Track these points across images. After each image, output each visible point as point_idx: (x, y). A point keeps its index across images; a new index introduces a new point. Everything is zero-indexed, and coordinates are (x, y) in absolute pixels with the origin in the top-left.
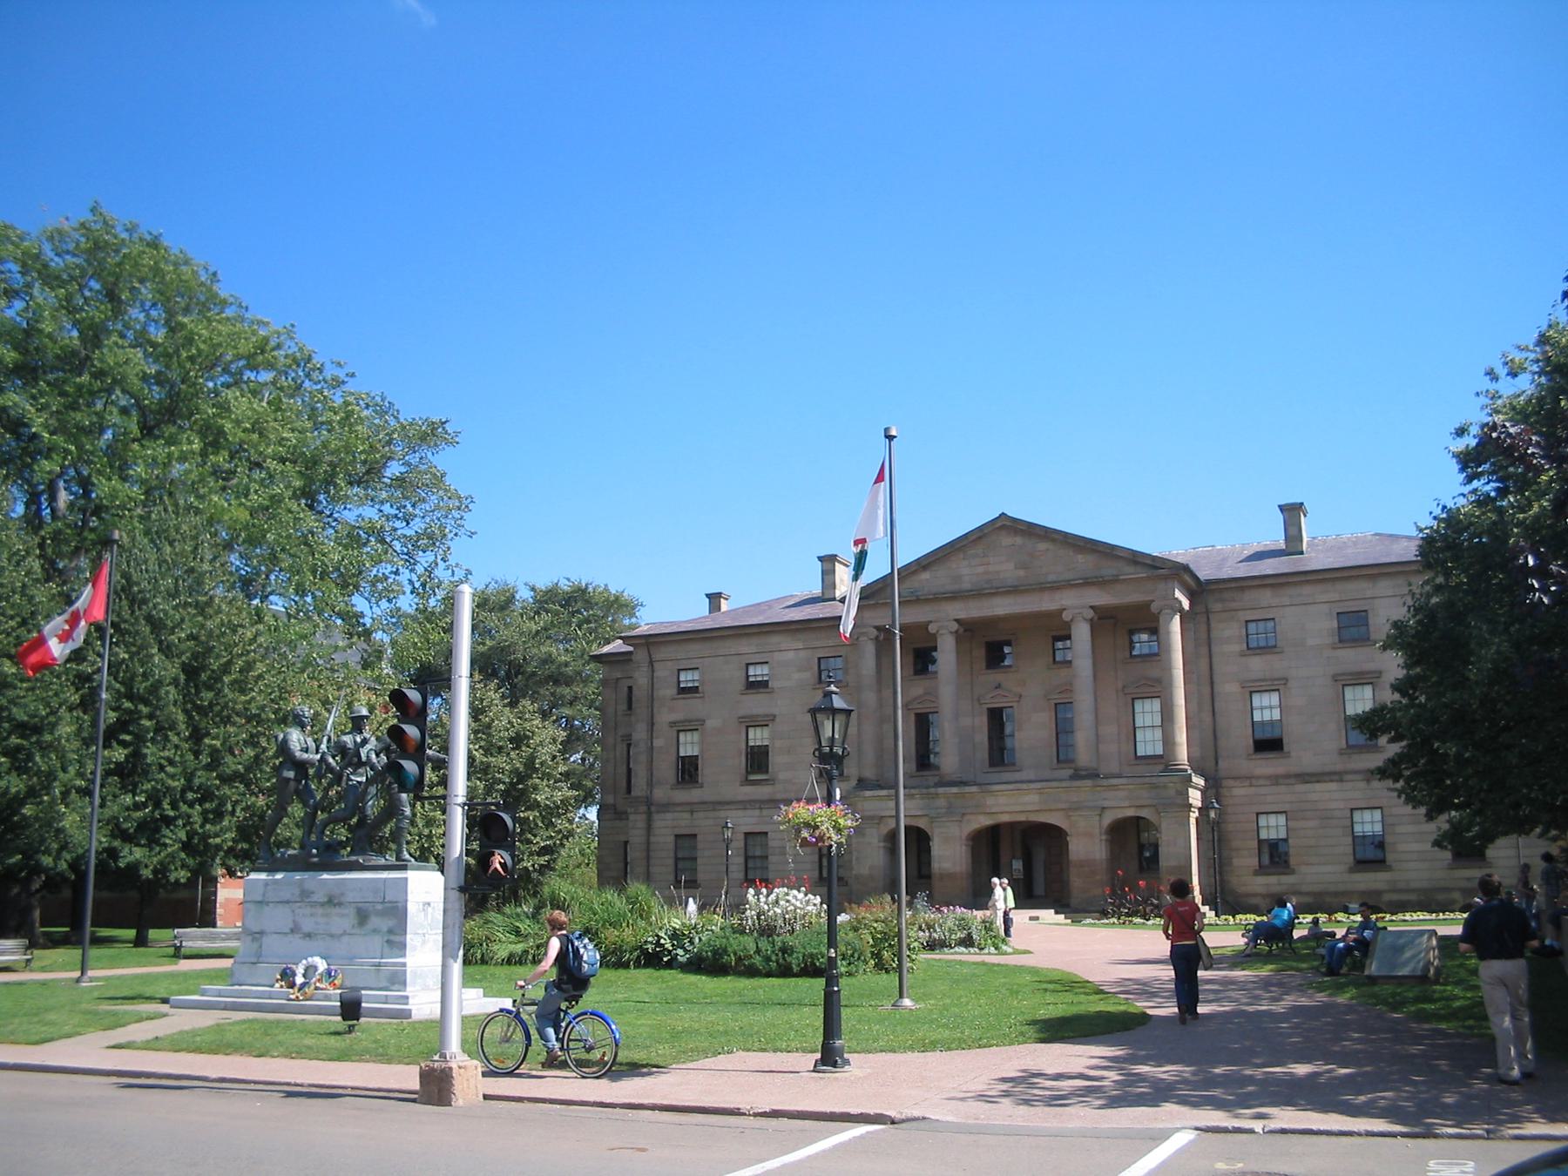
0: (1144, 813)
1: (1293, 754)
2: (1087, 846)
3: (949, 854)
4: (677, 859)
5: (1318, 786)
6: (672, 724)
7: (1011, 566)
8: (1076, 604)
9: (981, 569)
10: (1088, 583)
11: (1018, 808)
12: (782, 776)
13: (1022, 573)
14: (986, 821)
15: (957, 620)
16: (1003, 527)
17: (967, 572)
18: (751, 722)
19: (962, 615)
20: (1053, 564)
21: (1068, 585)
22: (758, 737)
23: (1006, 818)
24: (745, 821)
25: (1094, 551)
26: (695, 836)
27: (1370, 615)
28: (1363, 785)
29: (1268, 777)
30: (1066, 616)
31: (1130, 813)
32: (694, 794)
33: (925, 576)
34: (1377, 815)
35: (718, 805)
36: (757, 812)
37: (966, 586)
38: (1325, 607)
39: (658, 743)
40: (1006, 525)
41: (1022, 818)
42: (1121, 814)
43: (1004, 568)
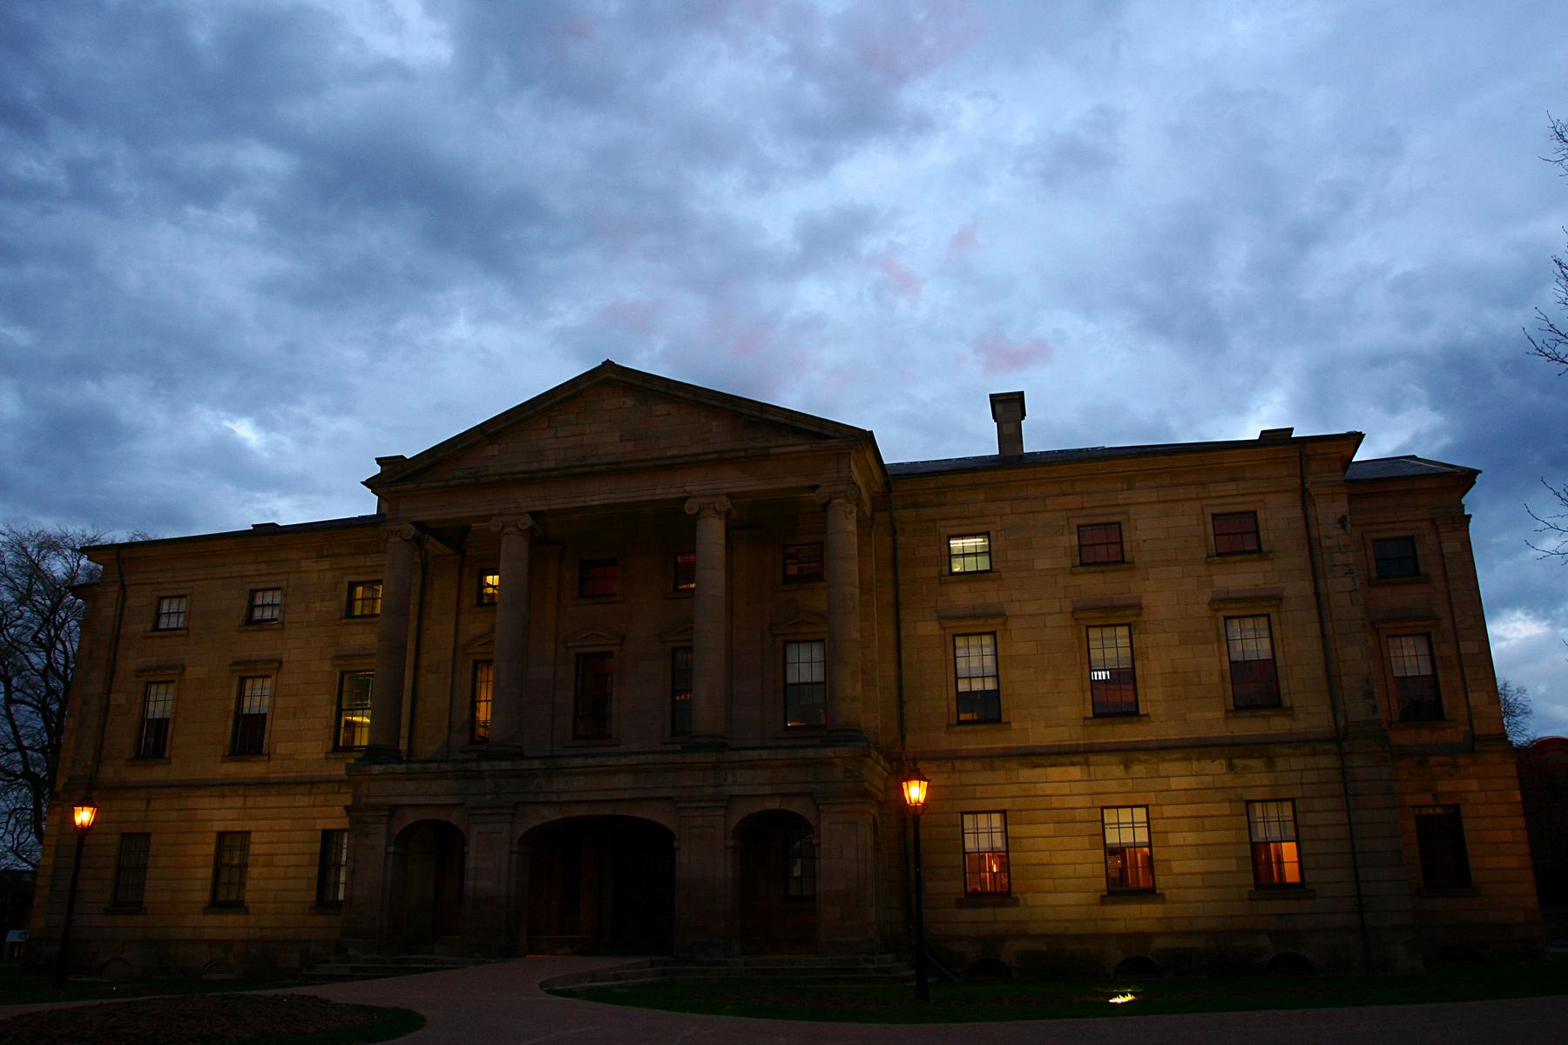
0: (795, 806)
2: (705, 861)
3: (490, 863)
6: (141, 671)
10: (721, 460)
11: (602, 796)
12: (281, 749)
14: (552, 815)
16: (608, 381)
22: (258, 699)
24: (221, 814)
26: (149, 835)
28: (1118, 771)
30: (690, 508)
31: (773, 805)
32: (158, 773)
33: (493, 450)
34: (1140, 814)
36: (239, 802)
39: (117, 699)
41: (606, 811)
42: (758, 807)
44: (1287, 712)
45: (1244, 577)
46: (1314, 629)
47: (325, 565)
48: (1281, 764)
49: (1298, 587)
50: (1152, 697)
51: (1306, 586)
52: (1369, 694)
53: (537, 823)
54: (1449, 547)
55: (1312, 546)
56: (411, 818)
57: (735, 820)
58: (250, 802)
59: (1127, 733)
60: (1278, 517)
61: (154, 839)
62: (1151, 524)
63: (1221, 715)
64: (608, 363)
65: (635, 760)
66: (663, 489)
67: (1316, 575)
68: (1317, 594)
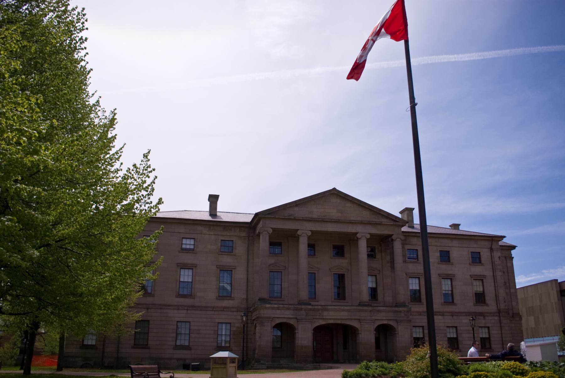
0: (391, 323)
2: (367, 336)
3: (304, 337)
4: (148, 333)
13: (340, 215)
14: (322, 322)
15: (311, 231)
17: (316, 211)
18: (185, 266)
19: (314, 229)
20: (354, 214)
21: (362, 223)
22: (186, 276)
23: (331, 322)
26: (148, 321)
27: (450, 253)
28: (451, 317)
29: (417, 312)
30: (358, 235)
31: (385, 322)
33: (296, 209)
35: (162, 306)
36: (185, 312)
37: (315, 216)
40: (334, 193)
41: (339, 322)
42: (381, 323)
43: (332, 210)
44: (487, 305)
45: (477, 270)
46: (493, 284)
47: (212, 233)
48: (487, 318)
49: (489, 273)
50: (457, 299)
51: (491, 273)
53: (318, 324)
54: (509, 265)
55: (493, 263)
56: (278, 321)
57: (376, 325)
58: (189, 312)
59: (451, 308)
60: (485, 255)
61: (151, 322)
62: (459, 253)
64: (334, 189)
65: (348, 308)
66: (350, 229)
67: (494, 270)
68: (494, 276)
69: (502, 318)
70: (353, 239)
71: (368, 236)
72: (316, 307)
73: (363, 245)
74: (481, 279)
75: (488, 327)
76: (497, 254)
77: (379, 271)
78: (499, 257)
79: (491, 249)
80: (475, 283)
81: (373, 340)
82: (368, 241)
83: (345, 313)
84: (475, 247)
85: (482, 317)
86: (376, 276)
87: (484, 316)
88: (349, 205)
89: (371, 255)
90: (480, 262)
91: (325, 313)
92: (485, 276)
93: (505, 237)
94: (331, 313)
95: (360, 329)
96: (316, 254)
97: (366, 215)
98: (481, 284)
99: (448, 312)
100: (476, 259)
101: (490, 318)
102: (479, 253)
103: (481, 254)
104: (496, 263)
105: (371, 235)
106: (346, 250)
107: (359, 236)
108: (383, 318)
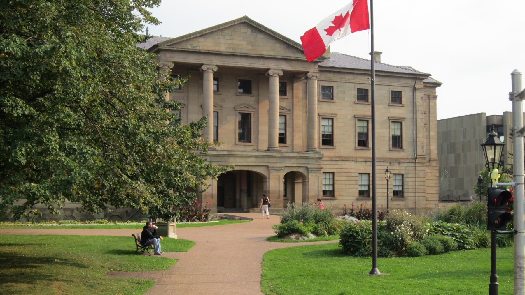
1: (337, 147)
2: (275, 184)
5: (347, 163)
7: (245, 43)
8: (277, 69)
9: (230, 42)
13: (250, 47)
15: (216, 65)
16: (244, 23)
23: (237, 168)
25: (285, 43)
28: (364, 163)
33: (201, 40)
37: (222, 49)
38: (352, 85)
40: (246, 23)
43: (242, 43)
52: (423, 147)
63: (388, 149)
64: (246, 17)
69: (417, 165)
70: (263, 76)
71: (281, 74)
72: (222, 153)
73: (276, 83)
74: (399, 122)
75: (403, 175)
76: (420, 95)
77: (290, 110)
78: (422, 98)
79: (414, 89)
80: (392, 126)
81: (282, 188)
82: (280, 78)
83: (253, 159)
84: (397, 85)
85: (397, 164)
86: (285, 116)
87: (399, 163)
88: (260, 36)
89: (283, 92)
90: (401, 103)
91: (231, 159)
92: (404, 119)
93: (430, 75)
94: (237, 159)
95: (267, 176)
96: (220, 90)
97: (279, 51)
98: (399, 127)
99: (361, 158)
100: (397, 98)
101: (405, 165)
102: (401, 92)
103: (403, 93)
104: (418, 104)
105: (285, 72)
106: (253, 86)
107: (270, 72)
108: (293, 165)
